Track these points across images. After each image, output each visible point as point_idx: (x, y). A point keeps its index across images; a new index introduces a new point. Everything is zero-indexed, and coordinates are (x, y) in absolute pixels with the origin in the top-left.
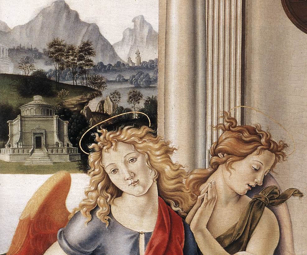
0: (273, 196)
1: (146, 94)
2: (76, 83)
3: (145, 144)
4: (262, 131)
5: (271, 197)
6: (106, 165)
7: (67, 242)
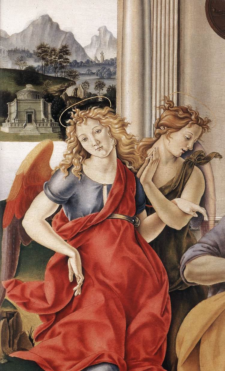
0: (200, 158)
1: (108, 83)
2: (57, 76)
3: (107, 119)
4: (192, 110)
5: (199, 159)
6: (79, 135)
7: (50, 191)
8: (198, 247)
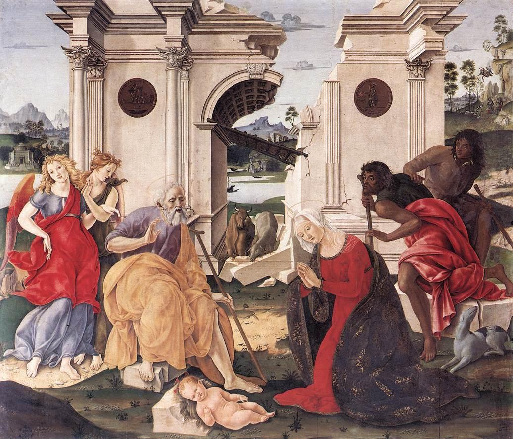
1: (65, 141)
8: (115, 232)
